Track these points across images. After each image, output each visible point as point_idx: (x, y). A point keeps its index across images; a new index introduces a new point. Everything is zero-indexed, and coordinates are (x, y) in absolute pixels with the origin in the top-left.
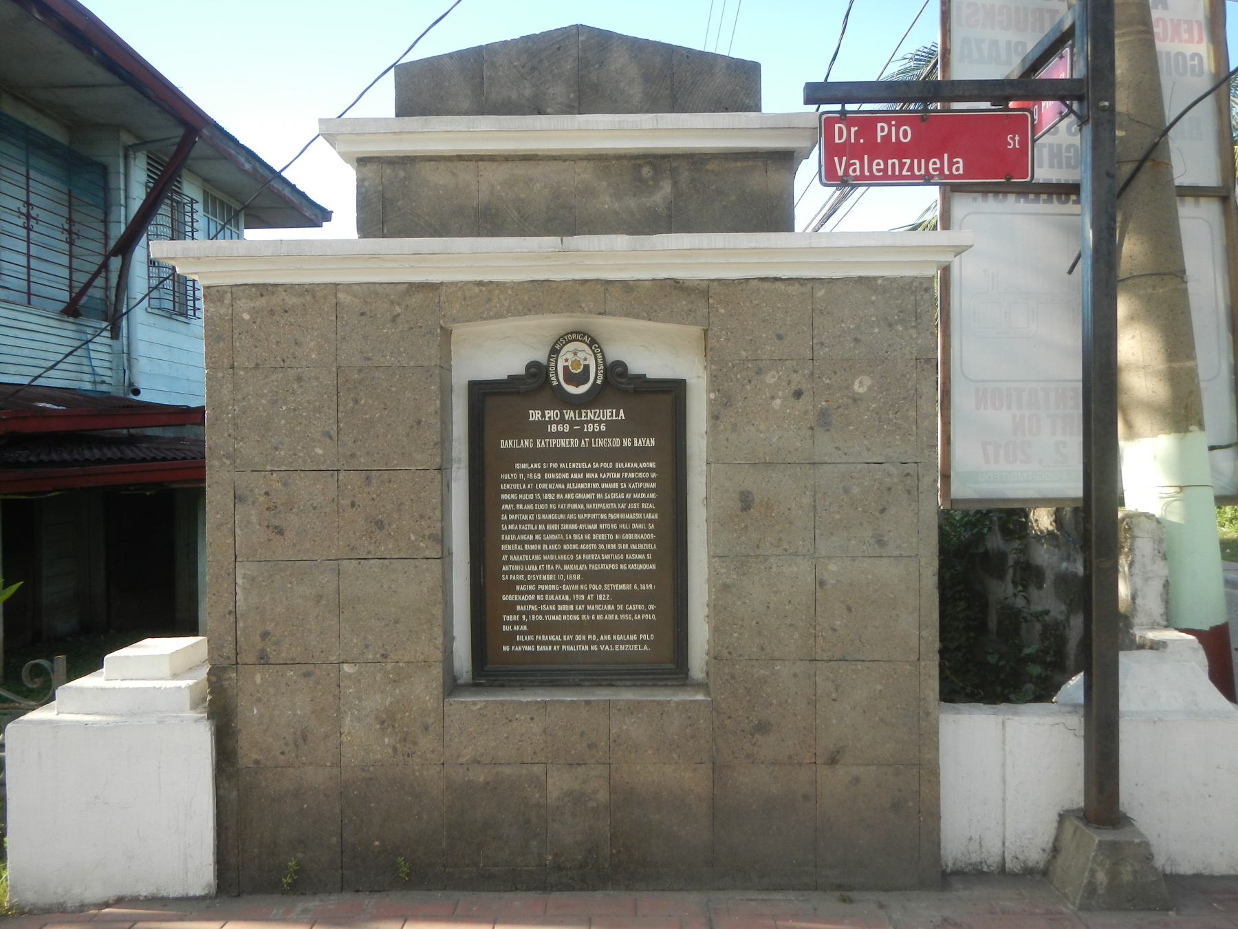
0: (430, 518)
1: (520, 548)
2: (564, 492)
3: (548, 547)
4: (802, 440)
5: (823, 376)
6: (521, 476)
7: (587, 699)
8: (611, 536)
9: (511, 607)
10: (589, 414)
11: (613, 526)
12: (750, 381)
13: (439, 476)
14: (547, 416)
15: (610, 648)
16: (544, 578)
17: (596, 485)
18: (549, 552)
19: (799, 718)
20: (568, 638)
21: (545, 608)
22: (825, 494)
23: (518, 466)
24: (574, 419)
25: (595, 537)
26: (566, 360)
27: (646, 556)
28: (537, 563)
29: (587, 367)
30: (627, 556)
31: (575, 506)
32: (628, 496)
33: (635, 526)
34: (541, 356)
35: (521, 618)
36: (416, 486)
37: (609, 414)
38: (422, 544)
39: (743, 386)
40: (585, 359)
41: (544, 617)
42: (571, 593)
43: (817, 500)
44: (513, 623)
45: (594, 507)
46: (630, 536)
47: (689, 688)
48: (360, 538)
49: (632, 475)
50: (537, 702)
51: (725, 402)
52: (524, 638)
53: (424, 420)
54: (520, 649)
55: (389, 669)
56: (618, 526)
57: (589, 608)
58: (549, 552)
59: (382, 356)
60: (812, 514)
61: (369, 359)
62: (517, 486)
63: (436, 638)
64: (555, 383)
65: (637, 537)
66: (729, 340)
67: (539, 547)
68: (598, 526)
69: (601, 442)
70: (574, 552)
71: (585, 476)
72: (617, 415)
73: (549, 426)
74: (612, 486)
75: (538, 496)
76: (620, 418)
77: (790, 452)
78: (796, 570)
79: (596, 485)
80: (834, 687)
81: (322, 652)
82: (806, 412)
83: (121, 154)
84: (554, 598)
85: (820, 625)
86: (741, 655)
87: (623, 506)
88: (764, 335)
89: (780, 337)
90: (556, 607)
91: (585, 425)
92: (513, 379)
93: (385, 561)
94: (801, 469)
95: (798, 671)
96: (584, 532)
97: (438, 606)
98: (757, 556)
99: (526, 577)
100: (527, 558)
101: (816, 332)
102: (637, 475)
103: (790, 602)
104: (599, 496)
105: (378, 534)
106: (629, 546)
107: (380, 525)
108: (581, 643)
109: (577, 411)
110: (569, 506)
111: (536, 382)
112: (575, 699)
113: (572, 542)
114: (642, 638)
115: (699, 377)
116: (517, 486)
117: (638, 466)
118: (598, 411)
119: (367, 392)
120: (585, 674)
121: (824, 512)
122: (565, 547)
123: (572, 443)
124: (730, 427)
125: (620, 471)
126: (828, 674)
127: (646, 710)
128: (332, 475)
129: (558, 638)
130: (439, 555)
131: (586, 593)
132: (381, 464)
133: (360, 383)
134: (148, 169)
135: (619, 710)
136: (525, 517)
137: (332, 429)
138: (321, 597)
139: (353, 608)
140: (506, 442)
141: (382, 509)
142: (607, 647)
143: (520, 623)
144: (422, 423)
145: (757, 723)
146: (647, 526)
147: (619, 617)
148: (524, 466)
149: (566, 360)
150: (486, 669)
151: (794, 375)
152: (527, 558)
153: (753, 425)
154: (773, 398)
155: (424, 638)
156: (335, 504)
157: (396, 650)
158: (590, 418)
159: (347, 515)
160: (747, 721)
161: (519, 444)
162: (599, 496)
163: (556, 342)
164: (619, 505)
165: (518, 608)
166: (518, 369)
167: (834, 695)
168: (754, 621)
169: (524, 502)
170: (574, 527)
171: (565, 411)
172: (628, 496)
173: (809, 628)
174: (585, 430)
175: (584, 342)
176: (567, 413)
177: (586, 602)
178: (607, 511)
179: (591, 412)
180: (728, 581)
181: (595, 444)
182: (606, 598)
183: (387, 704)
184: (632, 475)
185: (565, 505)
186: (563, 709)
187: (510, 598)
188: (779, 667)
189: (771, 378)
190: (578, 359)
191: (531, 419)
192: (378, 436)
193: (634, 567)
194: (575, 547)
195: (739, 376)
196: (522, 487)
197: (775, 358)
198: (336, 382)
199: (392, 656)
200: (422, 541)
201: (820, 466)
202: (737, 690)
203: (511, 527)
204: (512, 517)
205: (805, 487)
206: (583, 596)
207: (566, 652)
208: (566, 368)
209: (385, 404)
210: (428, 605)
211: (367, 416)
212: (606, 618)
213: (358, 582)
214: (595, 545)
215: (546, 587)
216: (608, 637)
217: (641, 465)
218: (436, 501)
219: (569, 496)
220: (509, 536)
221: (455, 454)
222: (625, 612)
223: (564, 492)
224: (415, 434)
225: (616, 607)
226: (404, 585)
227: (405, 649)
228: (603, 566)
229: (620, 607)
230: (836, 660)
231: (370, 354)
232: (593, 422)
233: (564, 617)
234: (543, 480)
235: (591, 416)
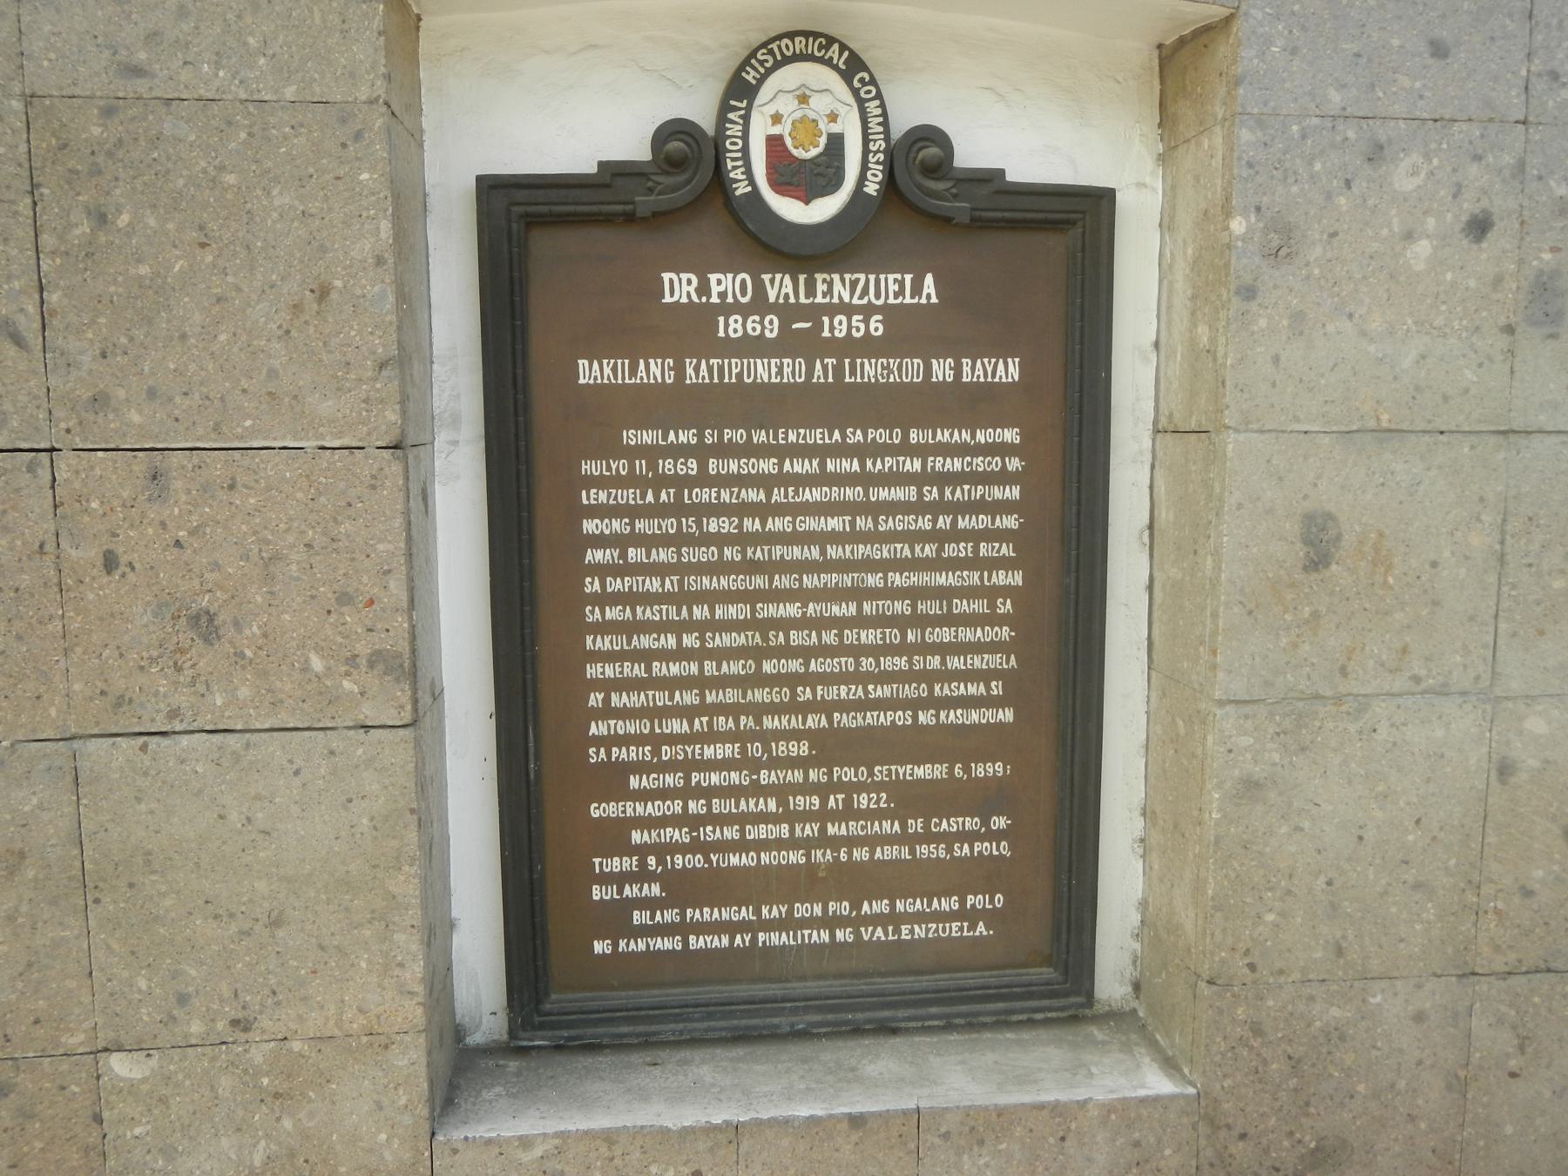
0: (371, 602)
1: (638, 671)
2: (763, 511)
3: (719, 668)
4: (1480, 365)
5: (1552, 173)
6: (641, 465)
7: (857, 1109)
8: (893, 636)
9: (614, 837)
10: (837, 286)
11: (901, 607)
12: (1348, 184)
13: (396, 468)
14: (715, 289)
15: (886, 934)
16: (709, 752)
17: (852, 493)
18: (722, 682)
19: (1423, 1126)
20: (775, 912)
21: (709, 833)
22: (1530, 519)
23: (630, 437)
24: (792, 300)
25: (850, 636)
26: (777, 119)
27: (988, 688)
28: (688, 713)
29: (836, 144)
30: (937, 688)
31: (796, 552)
32: (944, 522)
33: (962, 606)
34: (700, 110)
35: (643, 864)
36: (323, 499)
37: (893, 288)
38: (347, 684)
39: (1329, 196)
40: (833, 117)
41: (708, 860)
42: (781, 792)
43: (1508, 537)
44: (622, 879)
45: (848, 553)
46: (946, 635)
47: (1098, 1033)
48: (142, 668)
49: (956, 465)
50: (710, 1129)
51: (1275, 244)
52: (652, 918)
53: (338, 283)
54: (642, 946)
55: (259, 1059)
56: (914, 607)
57: (832, 830)
58: (722, 682)
59: (185, 63)
60: (1492, 578)
61: (137, 71)
62: (628, 496)
63: (401, 965)
64: (742, 189)
65: (967, 635)
66: (1294, 51)
67: (694, 668)
68: (860, 608)
69: (870, 370)
70: (792, 680)
71: (822, 465)
72: (917, 289)
73: (721, 319)
74: (898, 494)
75: (689, 524)
76: (924, 301)
77: (1446, 398)
78: (1440, 733)
79: (852, 493)
80: (1516, 1042)
81: (37, 1022)
82: (1498, 281)
84: (737, 807)
85: (1492, 881)
86: (1281, 972)
87: (929, 550)
88: (1396, 42)
89: (1439, 50)
90: (742, 831)
91: (826, 320)
92: (614, 173)
93: (231, 739)
94: (1472, 447)
95: (1428, 1005)
96: (820, 624)
97: (406, 868)
98: (1338, 700)
99: (656, 752)
100: (661, 699)
101: (1540, 37)
102: (970, 464)
103: (1418, 822)
104: (864, 523)
105: (201, 656)
106: (943, 662)
107: (205, 625)
108: (811, 923)
109: (802, 278)
110: (778, 551)
111: (688, 182)
112: (819, 1112)
113: (787, 652)
114: (973, 906)
115: (1141, 185)
116: (628, 496)
117: (973, 436)
118: (862, 277)
119: (138, 184)
120: (820, 1010)
121: (1525, 570)
122: (768, 667)
123: (787, 370)
124: (1285, 322)
125: (922, 451)
126: (1504, 1009)
127: (1019, 1131)
128: (31, 468)
129: (746, 913)
130: (407, 717)
131: (823, 791)
132: (201, 431)
133: (110, 154)
135: (946, 1136)
136: (653, 585)
137: (22, 310)
138: (22, 855)
139: (131, 885)
140: (596, 365)
141: (210, 577)
142: (879, 932)
143: (642, 876)
144: (334, 296)
145: (1313, 1145)
146: (992, 605)
147: (912, 852)
148: (647, 437)
149: (777, 119)
150: (547, 1007)
151: (1474, 170)
152: (661, 699)
153: (1351, 316)
154: (1409, 236)
155: (363, 965)
156: (49, 560)
157: (278, 1004)
158: (840, 297)
159: (91, 596)
160: (1286, 1143)
161: (633, 371)
162: (864, 523)
163: (746, 62)
164: (917, 549)
165: (636, 837)
166: (633, 146)
167: (1513, 1064)
168: (1322, 879)
169: (648, 542)
170: (792, 610)
171: (766, 277)
172: (944, 522)
173: (1464, 890)
174: (826, 334)
175: (828, 63)
176: (772, 281)
177: (824, 816)
178: (884, 566)
179: (843, 281)
180: (1259, 772)
181: (853, 373)
182: (878, 802)
183: (258, 1159)
184: (956, 465)
185: (766, 548)
186: (785, 1142)
187: (612, 809)
188: (1379, 999)
189: (1405, 177)
190: (812, 115)
191: (667, 299)
192: (183, 337)
193: (953, 717)
194: (795, 666)
195: (1318, 167)
196: (643, 497)
197: (1425, 115)
198: (23, 148)
199: (264, 1022)
200: (348, 674)
201: (1522, 441)
202: (1265, 1062)
203: (612, 613)
204: (615, 585)
205: (1482, 499)
206: (816, 800)
207: (768, 950)
208: (774, 143)
209: (201, 228)
210: (374, 867)
211: (144, 270)
212: (878, 854)
213: (143, 807)
214: (851, 659)
215: (715, 778)
216: (881, 906)
217: (981, 437)
218: (390, 546)
219: (777, 524)
220: (607, 640)
221: (440, 400)
222: (928, 837)
223: (763, 511)
224: (312, 330)
225: (904, 826)
226: (295, 809)
227: (304, 999)
228: (872, 718)
229: (915, 825)
230: (1527, 972)
231: (143, 56)
232: (848, 310)
233: (765, 858)
234: (703, 479)
235: (841, 291)
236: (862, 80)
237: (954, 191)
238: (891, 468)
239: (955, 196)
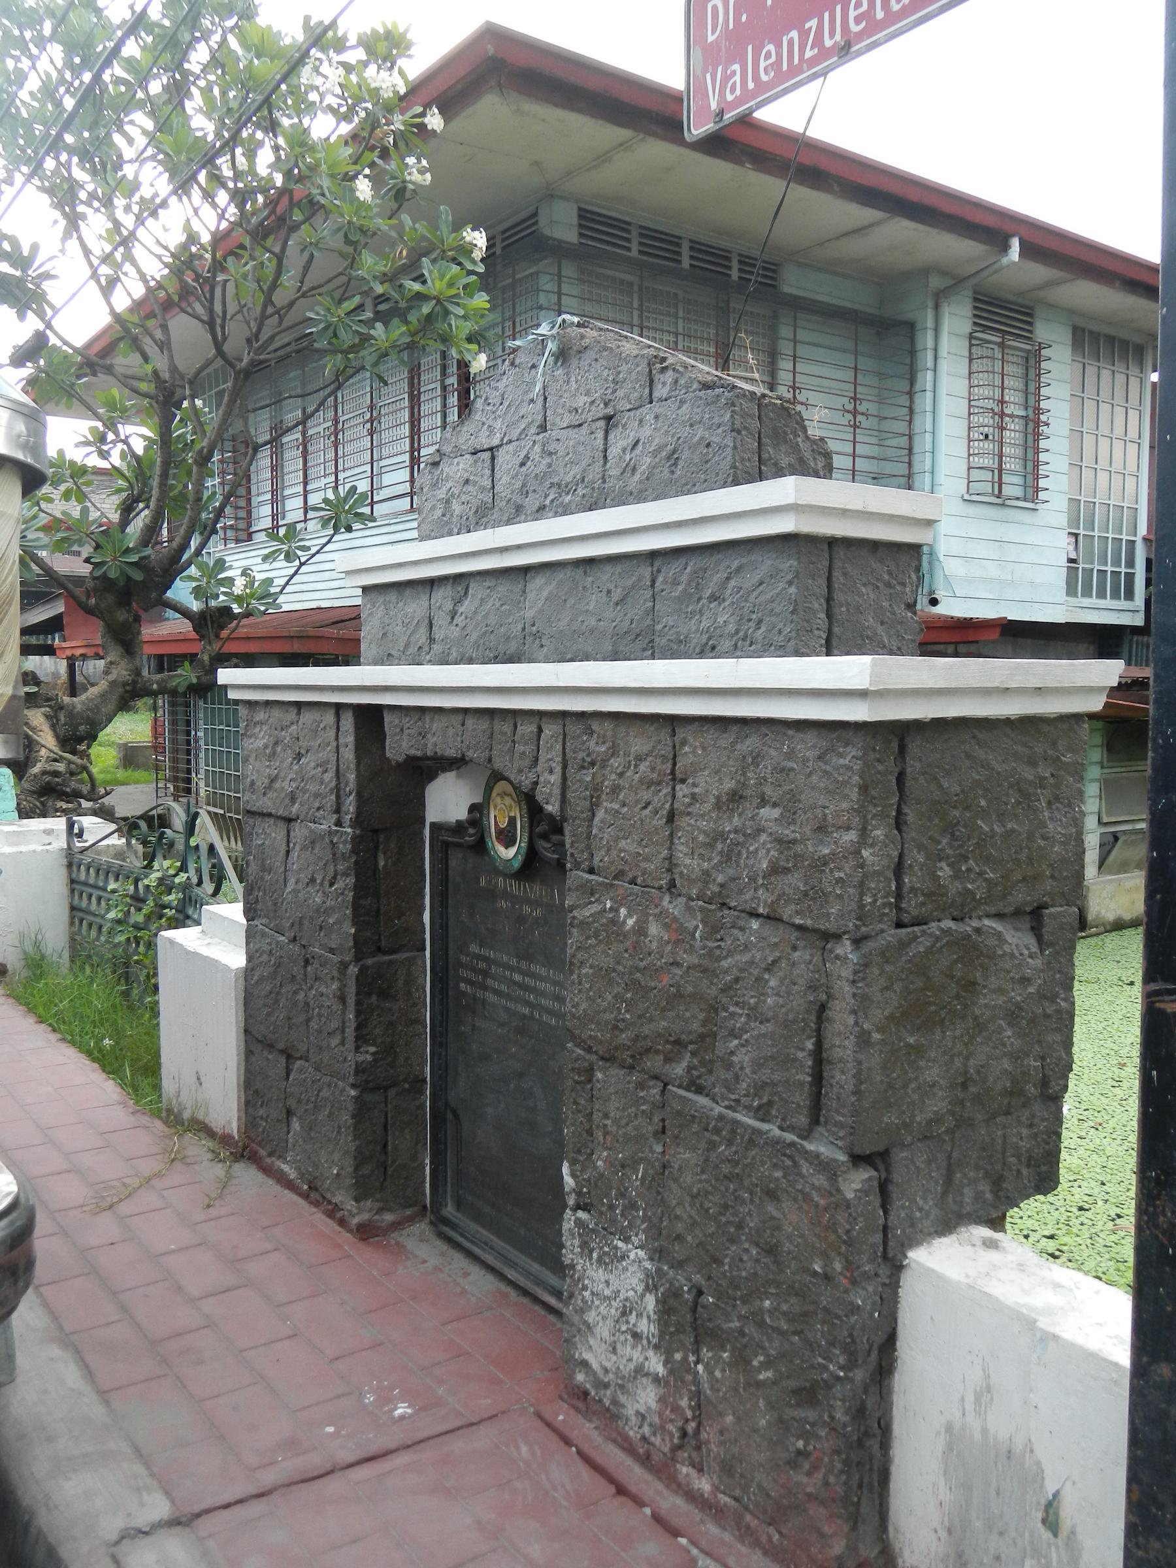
83: (930, 304)
134: (975, 316)
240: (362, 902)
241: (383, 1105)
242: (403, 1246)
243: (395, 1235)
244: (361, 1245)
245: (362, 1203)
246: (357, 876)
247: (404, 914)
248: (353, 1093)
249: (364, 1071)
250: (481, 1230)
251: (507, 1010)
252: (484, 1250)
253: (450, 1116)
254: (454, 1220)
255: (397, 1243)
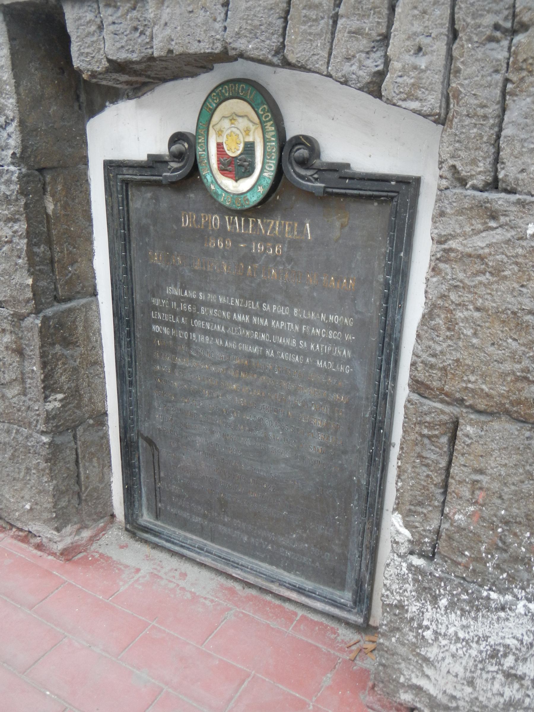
29: (249, 148)
148: (177, 292)
208: (220, 146)
236: (263, 110)
237: (316, 176)
238: (283, 327)
239: (316, 179)
240: (36, 249)
241: (73, 444)
242: (109, 558)
243: (94, 546)
244: (68, 566)
245: (64, 531)
246: (28, 220)
247: (77, 262)
248: (45, 439)
249: (54, 418)
250: (189, 535)
251: (222, 348)
252: (199, 553)
253: (142, 443)
254: (157, 529)
255: (102, 555)
